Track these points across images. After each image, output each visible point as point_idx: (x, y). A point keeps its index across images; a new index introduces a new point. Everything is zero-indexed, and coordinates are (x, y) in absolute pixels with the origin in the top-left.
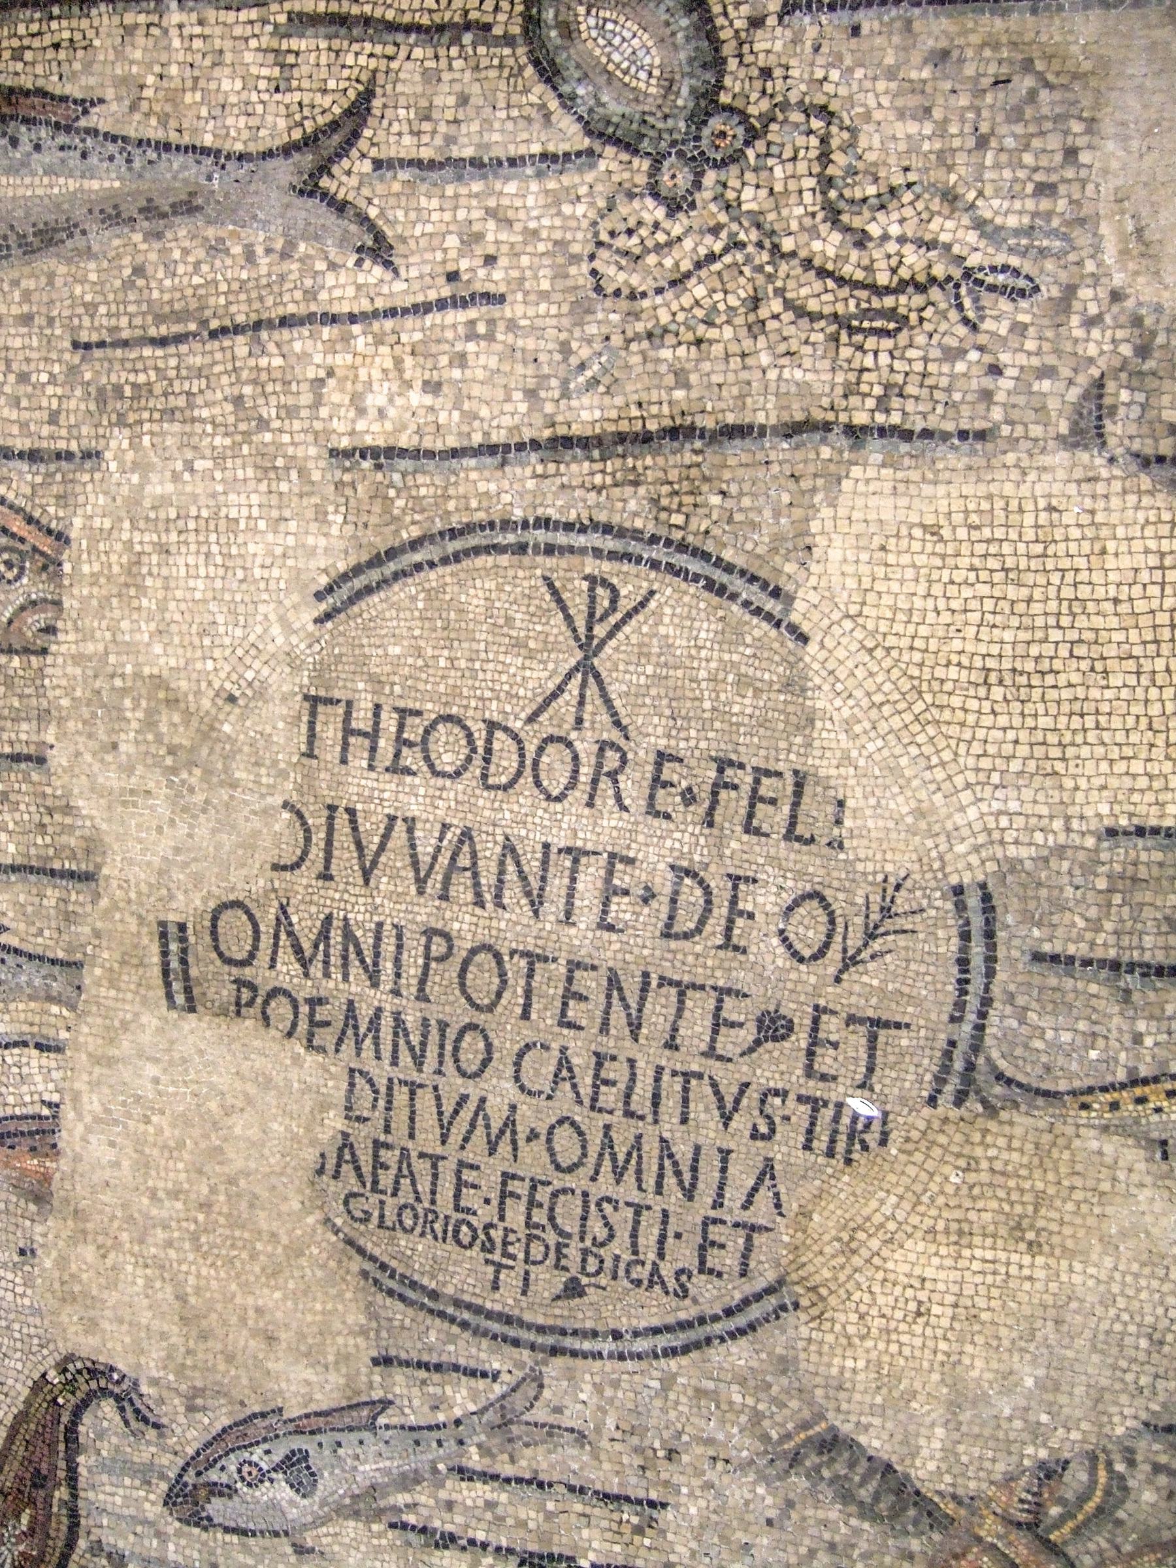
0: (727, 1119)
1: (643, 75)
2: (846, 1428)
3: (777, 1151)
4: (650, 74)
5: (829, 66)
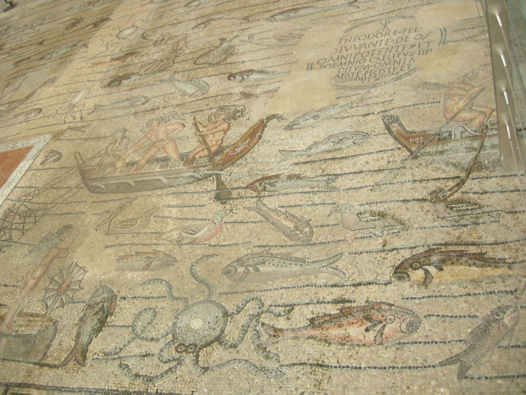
0: (405, 56)
2: (427, 81)
3: (414, 57)
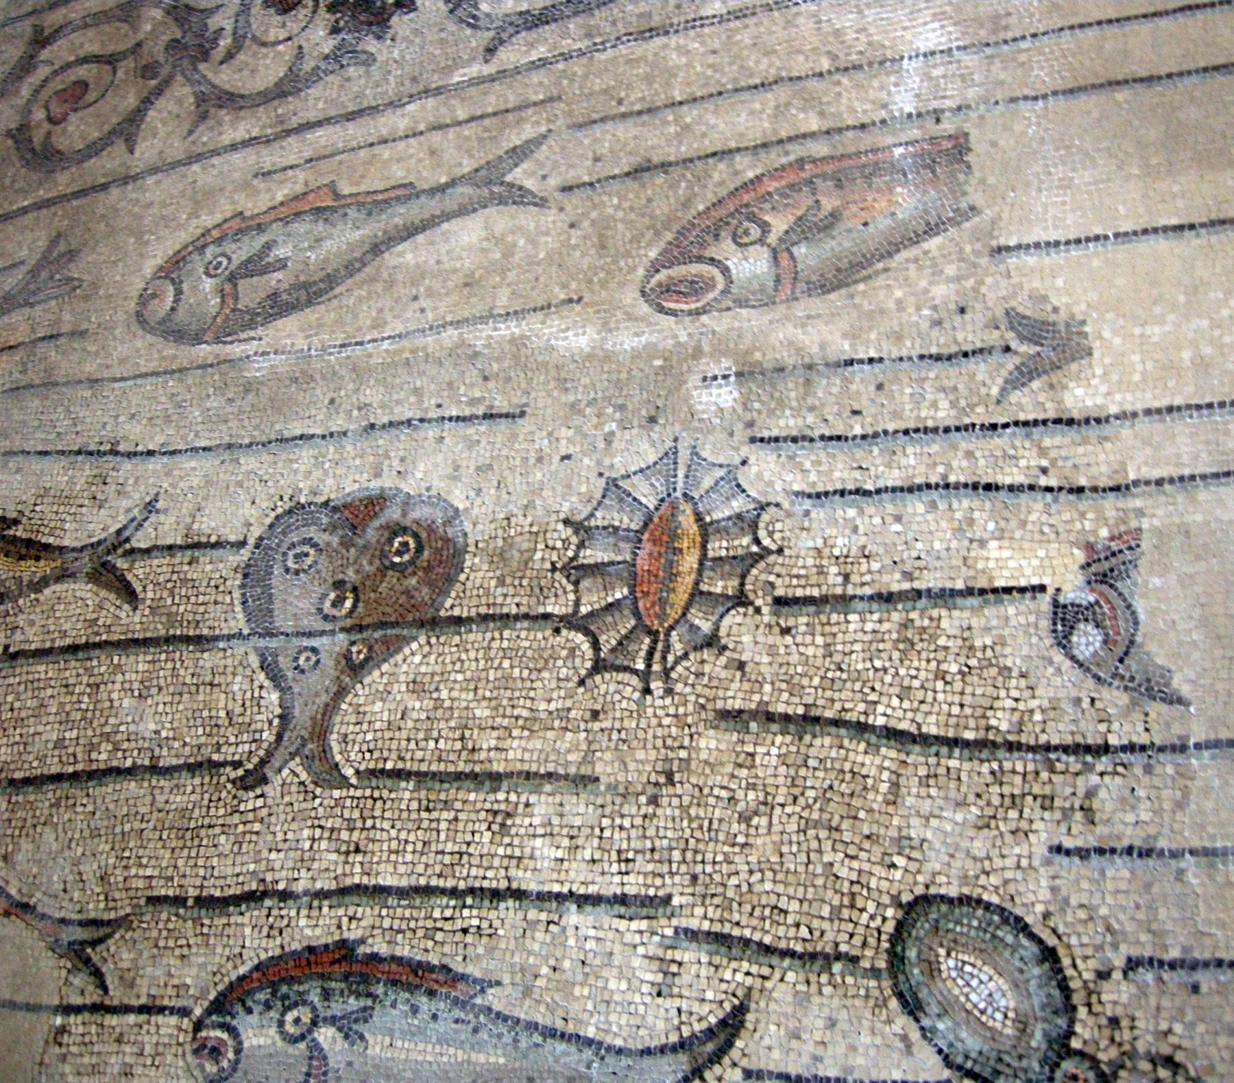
1: (999, 1016)
4: (1006, 1016)
5: (1173, 1019)
